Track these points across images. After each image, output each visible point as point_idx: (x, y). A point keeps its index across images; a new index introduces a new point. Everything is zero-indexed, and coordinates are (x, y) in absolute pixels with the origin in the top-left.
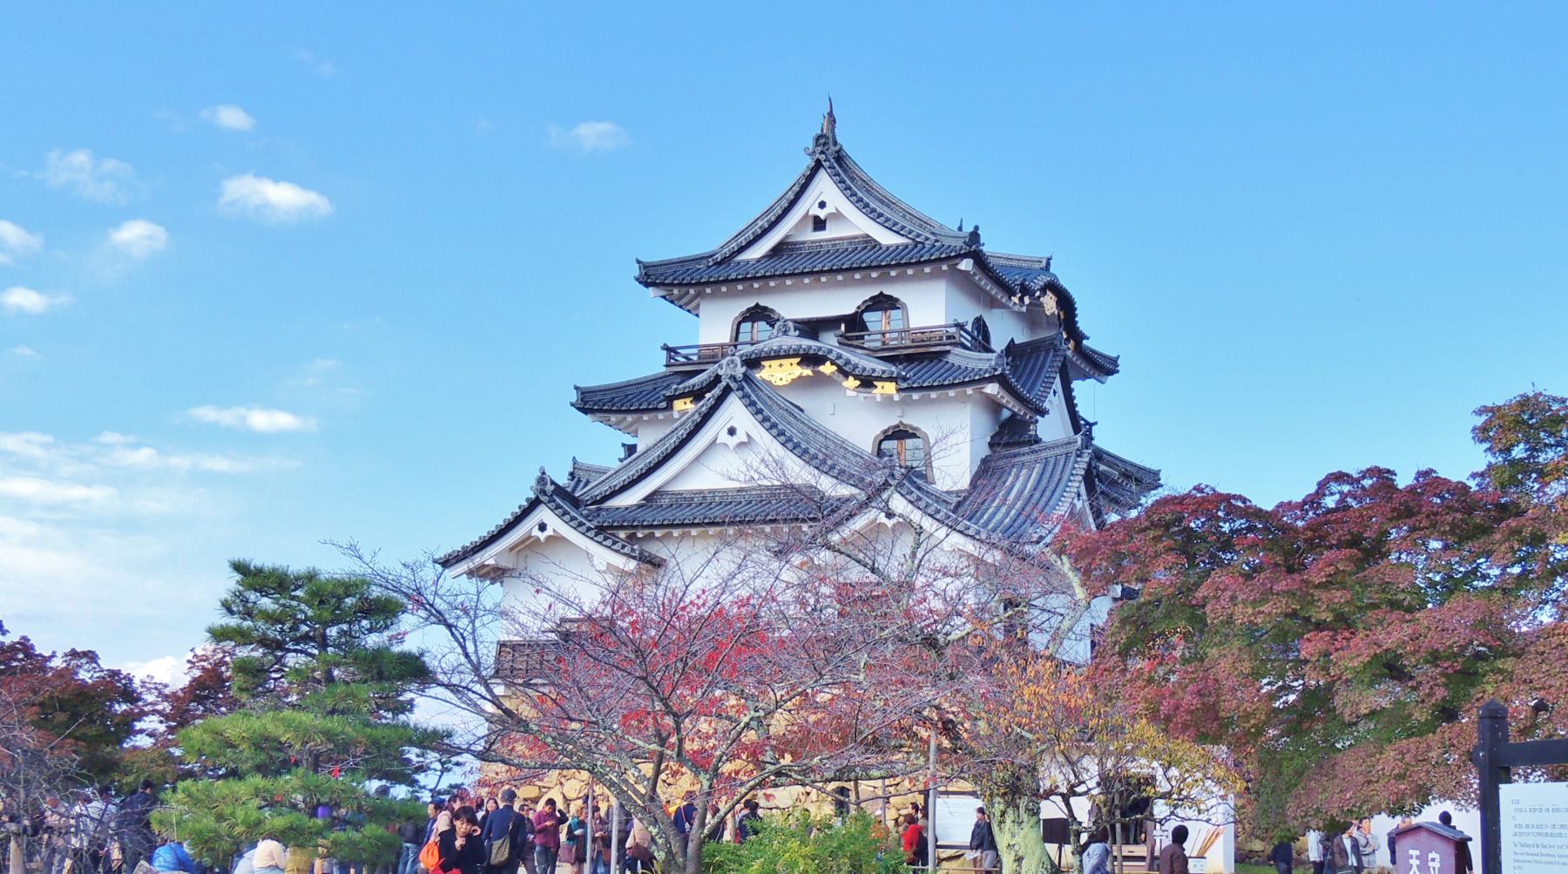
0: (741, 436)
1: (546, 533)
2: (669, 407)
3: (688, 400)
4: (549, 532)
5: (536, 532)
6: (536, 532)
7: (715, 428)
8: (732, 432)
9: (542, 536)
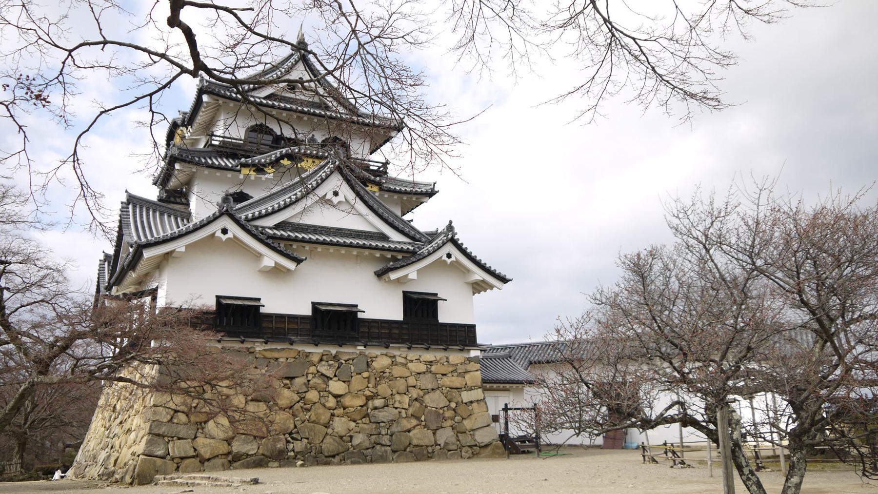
0: (340, 198)
1: (227, 236)
2: (240, 171)
4: (230, 235)
5: (219, 234)
6: (219, 234)
7: (326, 190)
8: (336, 194)
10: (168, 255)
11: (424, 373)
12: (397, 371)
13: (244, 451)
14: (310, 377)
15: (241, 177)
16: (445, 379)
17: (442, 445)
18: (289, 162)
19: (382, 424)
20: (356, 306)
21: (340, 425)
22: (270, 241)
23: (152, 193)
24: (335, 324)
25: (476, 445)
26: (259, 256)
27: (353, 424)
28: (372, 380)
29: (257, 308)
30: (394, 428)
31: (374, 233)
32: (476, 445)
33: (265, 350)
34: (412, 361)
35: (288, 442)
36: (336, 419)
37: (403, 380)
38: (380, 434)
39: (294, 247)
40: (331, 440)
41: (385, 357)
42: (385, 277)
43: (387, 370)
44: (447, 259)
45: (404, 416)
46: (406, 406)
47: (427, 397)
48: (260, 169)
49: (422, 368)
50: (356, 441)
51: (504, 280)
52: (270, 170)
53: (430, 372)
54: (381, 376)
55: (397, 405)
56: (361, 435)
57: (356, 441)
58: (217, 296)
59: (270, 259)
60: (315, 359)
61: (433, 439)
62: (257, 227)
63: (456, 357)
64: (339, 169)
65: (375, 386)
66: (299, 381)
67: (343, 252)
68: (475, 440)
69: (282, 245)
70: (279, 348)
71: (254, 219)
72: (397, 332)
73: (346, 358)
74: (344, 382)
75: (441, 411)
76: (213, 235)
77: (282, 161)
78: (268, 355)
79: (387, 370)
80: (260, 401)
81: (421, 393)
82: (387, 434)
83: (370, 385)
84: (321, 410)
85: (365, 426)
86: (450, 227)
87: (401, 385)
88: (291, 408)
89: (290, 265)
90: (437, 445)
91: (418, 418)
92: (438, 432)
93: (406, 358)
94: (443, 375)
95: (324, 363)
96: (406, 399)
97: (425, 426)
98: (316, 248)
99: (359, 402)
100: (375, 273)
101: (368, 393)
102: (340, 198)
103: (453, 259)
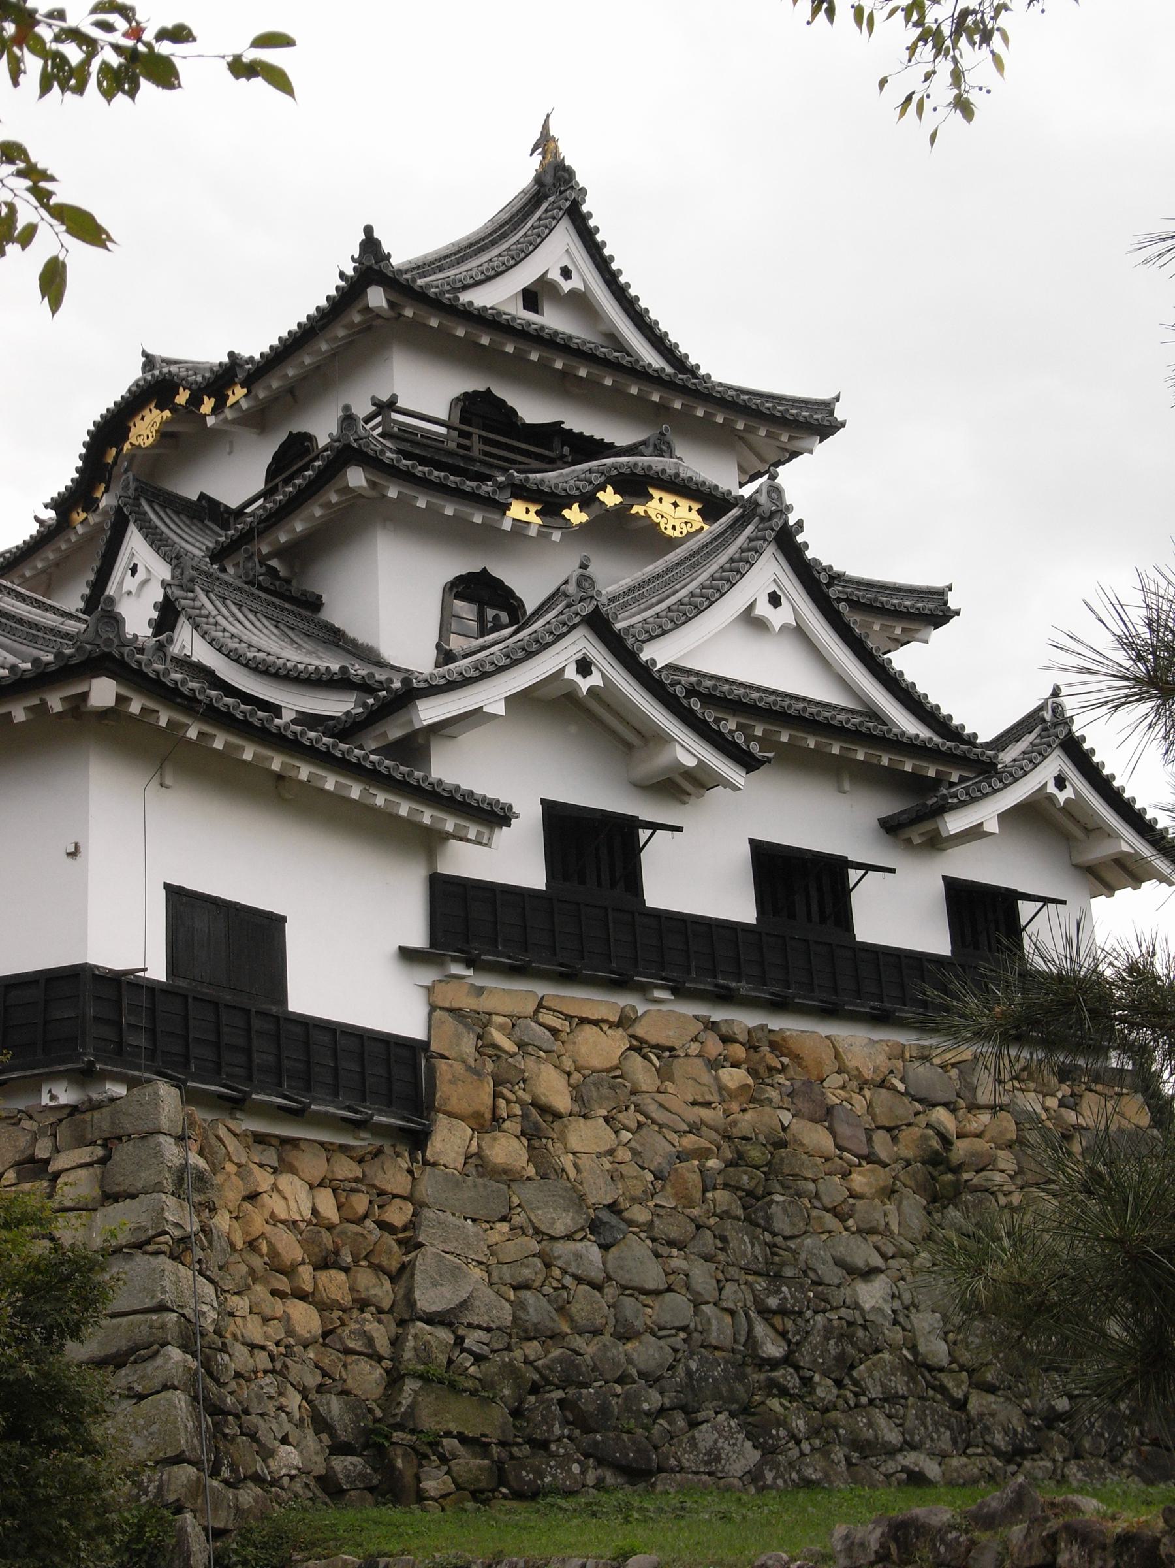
9: (584, 684)
22: (695, 704)
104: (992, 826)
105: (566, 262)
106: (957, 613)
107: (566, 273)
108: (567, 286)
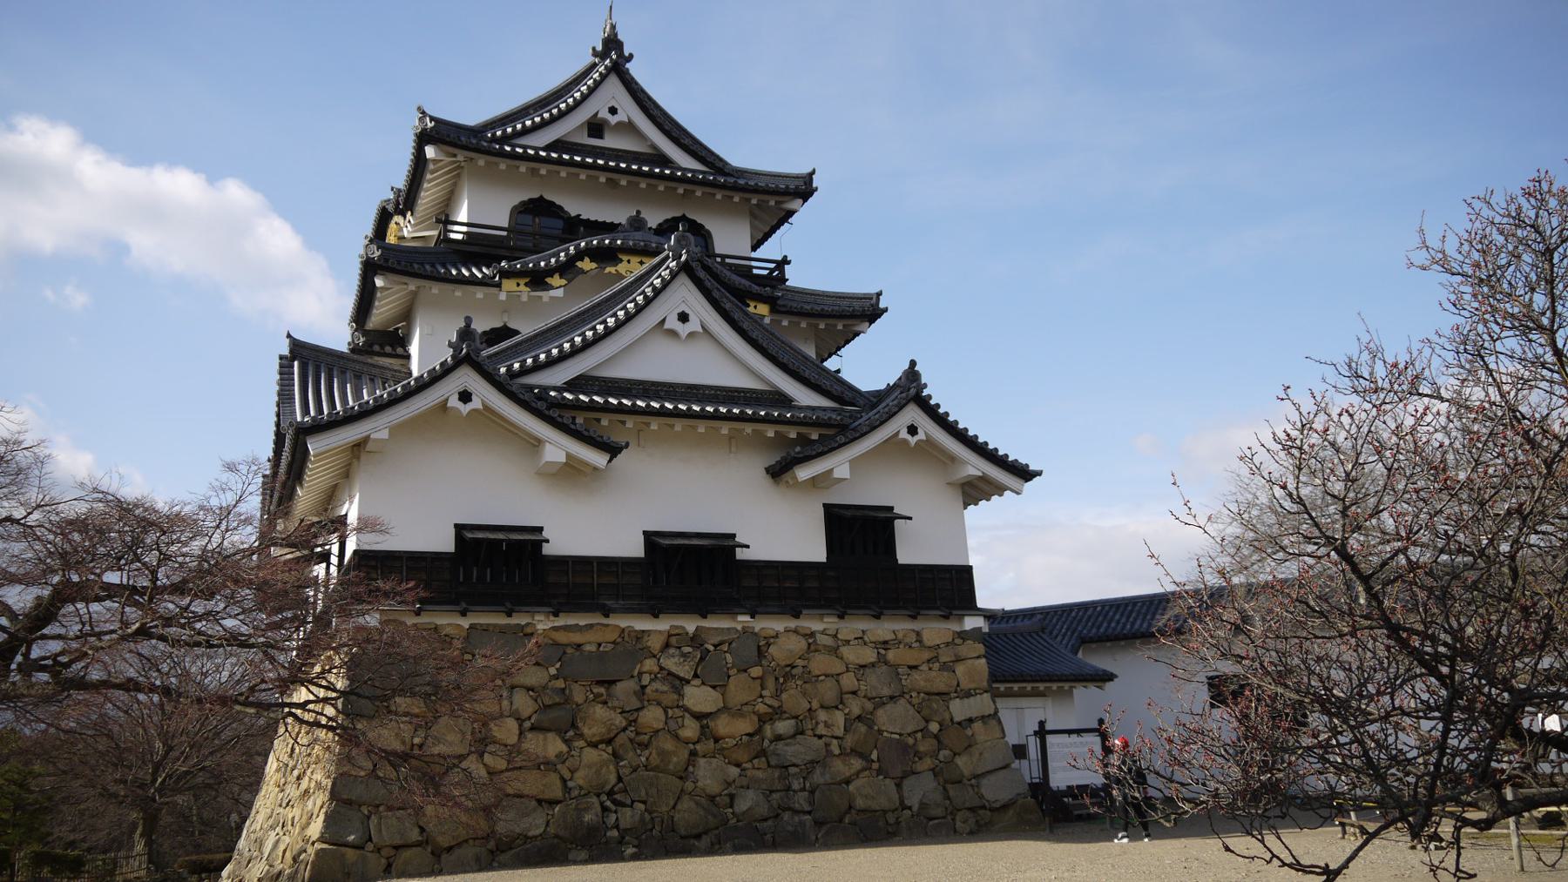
0: (693, 325)
2: (499, 285)
3: (522, 282)
4: (476, 404)
6: (454, 402)
7: (667, 308)
8: (683, 318)
10: (359, 447)
11: (873, 665)
12: (820, 663)
13: (518, 830)
14: (646, 679)
15: (503, 296)
16: (916, 675)
17: (915, 808)
18: (594, 265)
19: (792, 770)
20: (734, 536)
21: (709, 775)
22: (554, 413)
23: (337, 334)
24: (689, 570)
25: (983, 807)
26: (537, 443)
27: (734, 771)
28: (770, 683)
29: (538, 544)
30: (818, 777)
31: (762, 392)
32: (983, 807)
33: (554, 629)
34: (848, 642)
35: (605, 809)
36: (702, 761)
37: (830, 683)
38: (788, 789)
39: (605, 422)
40: (692, 804)
41: (794, 637)
42: (787, 477)
43: (800, 662)
44: (909, 437)
45: (837, 752)
46: (840, 732)
47: (880, 712)
48: (538, 280)
49: (869, 655)
50: (742, 805)
51: (1025, 474)
52: (556, 281)
53: (886, 663)
54: (787, 673)
55: (821, 730)
56: (751, 794)
57: (742, 805)
58: (456, 526)
59: (558, 447)
60: (655, 644)
61: (896, 797)
62: (531, 388)
63: (935, 630)
64: (686, 268)
65: (777, 696)
66: (624, 688)
67: (701, 430)
68: (982, 797)
69: (579, 421)
70: (582, 623)
71: (525, 371)
72: (815, 584)
73: (716, 640)
74: (714, 687)
75: (911, 741)
76: (443, 406)
77: (579, 264)
78: (562, 638)
79: (800, 662)
80: (549, 730)
81: (869, 706)
82: (803, 789)
83: (765, 693)
84: (668, 744)
85: (760, 774)
86: (912, 374)
87: (828, 691)
88: (609, 742)
89: (598, 459)
90: (904, 807)
91: (864, 756)
92: (907, 783)
93: (835, 636)
94: (911, 667)
95: (672, 651)
96: (839, 718)
97: (879, 772)
98: (648, 425)
99: (745, 726)
100: (767, 470)
101: (761, 708)
102: (693, 325)
103: (921, 436)
104: (842, 472)
105: (613, 103)
106: (886, 310)
107: (613, 111)
108: (613, 120)
